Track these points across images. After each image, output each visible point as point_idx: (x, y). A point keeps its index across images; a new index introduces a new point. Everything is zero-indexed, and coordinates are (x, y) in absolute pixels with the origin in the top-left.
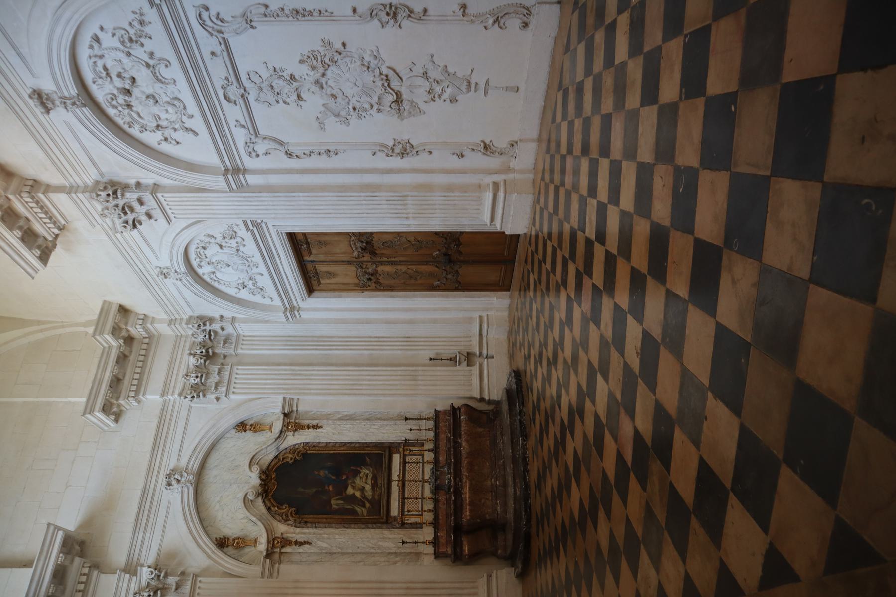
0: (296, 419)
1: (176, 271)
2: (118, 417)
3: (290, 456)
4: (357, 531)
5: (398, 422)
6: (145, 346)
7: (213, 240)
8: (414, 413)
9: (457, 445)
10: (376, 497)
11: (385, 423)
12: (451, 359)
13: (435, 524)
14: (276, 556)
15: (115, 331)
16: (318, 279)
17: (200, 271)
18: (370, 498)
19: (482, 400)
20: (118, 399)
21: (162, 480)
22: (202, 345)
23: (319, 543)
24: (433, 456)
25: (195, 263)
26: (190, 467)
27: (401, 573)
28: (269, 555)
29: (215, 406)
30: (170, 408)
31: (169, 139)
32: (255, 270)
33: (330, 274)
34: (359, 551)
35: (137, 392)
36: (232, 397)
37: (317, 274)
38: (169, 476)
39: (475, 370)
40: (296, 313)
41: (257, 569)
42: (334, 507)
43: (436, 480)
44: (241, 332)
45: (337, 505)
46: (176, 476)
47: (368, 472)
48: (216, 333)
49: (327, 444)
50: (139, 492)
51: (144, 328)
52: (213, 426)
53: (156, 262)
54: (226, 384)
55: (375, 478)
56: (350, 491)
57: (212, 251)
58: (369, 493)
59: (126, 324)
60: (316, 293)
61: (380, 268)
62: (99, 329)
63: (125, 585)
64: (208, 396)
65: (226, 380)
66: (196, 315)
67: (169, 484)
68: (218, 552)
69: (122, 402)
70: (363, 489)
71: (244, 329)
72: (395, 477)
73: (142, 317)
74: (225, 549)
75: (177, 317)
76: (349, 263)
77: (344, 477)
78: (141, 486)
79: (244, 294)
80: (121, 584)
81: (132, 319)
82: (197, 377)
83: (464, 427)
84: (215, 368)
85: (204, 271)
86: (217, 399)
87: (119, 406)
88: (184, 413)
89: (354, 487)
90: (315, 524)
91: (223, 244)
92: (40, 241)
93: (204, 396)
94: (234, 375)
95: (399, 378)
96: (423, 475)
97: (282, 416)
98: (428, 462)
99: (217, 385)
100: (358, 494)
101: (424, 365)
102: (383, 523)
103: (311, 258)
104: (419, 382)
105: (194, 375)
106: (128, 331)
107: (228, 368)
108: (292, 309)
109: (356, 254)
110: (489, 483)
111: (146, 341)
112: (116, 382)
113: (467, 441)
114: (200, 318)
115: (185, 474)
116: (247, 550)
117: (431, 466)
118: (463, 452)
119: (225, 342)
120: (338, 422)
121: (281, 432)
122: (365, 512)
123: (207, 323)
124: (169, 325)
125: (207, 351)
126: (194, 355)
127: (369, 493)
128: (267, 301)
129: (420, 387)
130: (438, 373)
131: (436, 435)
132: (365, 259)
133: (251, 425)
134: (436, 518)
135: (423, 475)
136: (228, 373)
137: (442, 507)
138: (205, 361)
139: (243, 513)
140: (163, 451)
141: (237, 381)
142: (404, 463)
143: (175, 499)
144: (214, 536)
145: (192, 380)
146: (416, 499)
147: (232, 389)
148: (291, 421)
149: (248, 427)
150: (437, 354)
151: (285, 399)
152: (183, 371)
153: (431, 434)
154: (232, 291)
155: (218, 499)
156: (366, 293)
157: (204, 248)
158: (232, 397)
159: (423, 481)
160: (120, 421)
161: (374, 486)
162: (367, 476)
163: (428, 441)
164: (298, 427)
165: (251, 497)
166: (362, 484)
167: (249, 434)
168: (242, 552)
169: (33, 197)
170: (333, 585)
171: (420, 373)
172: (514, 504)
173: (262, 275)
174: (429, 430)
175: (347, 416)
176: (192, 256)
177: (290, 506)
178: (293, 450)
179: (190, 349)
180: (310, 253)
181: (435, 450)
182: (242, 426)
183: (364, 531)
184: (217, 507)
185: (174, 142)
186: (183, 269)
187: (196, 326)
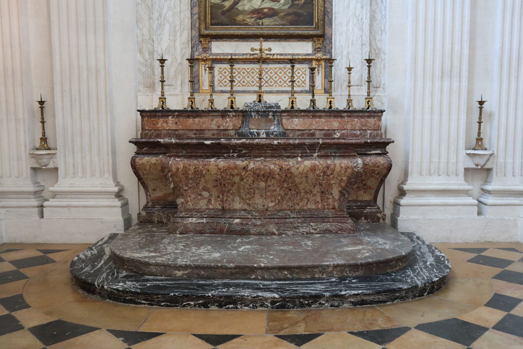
5: (367, 49)
8: (383, 73)
9: (306, 149)
10: (240, 18)
11: (366, 27)
12: (479, 139)
13: (193, 113)
19: (402, 193)
24: (302, 108)
39: (458, 182)
43: (257, 112)
55: (273, 13)
72: (277, 48)
83: (340, 163)
95: (448, 47)
96: (271, 92)
101: (470, 92)
104: (437, 84)
110: (237, 205)
113: (313, 169)
118: (291, 162)
129: (429, 85)
130: (454, 117)
131: (337, 114)
135: (271, 92)
137: (213, 124)
142: (292, 61)
146: (232, 81)
150: (491, 115)
153: (340, 104)
171: (456, 84)
172: (157, 265)
174: (349, 101)
181: (313, 112)
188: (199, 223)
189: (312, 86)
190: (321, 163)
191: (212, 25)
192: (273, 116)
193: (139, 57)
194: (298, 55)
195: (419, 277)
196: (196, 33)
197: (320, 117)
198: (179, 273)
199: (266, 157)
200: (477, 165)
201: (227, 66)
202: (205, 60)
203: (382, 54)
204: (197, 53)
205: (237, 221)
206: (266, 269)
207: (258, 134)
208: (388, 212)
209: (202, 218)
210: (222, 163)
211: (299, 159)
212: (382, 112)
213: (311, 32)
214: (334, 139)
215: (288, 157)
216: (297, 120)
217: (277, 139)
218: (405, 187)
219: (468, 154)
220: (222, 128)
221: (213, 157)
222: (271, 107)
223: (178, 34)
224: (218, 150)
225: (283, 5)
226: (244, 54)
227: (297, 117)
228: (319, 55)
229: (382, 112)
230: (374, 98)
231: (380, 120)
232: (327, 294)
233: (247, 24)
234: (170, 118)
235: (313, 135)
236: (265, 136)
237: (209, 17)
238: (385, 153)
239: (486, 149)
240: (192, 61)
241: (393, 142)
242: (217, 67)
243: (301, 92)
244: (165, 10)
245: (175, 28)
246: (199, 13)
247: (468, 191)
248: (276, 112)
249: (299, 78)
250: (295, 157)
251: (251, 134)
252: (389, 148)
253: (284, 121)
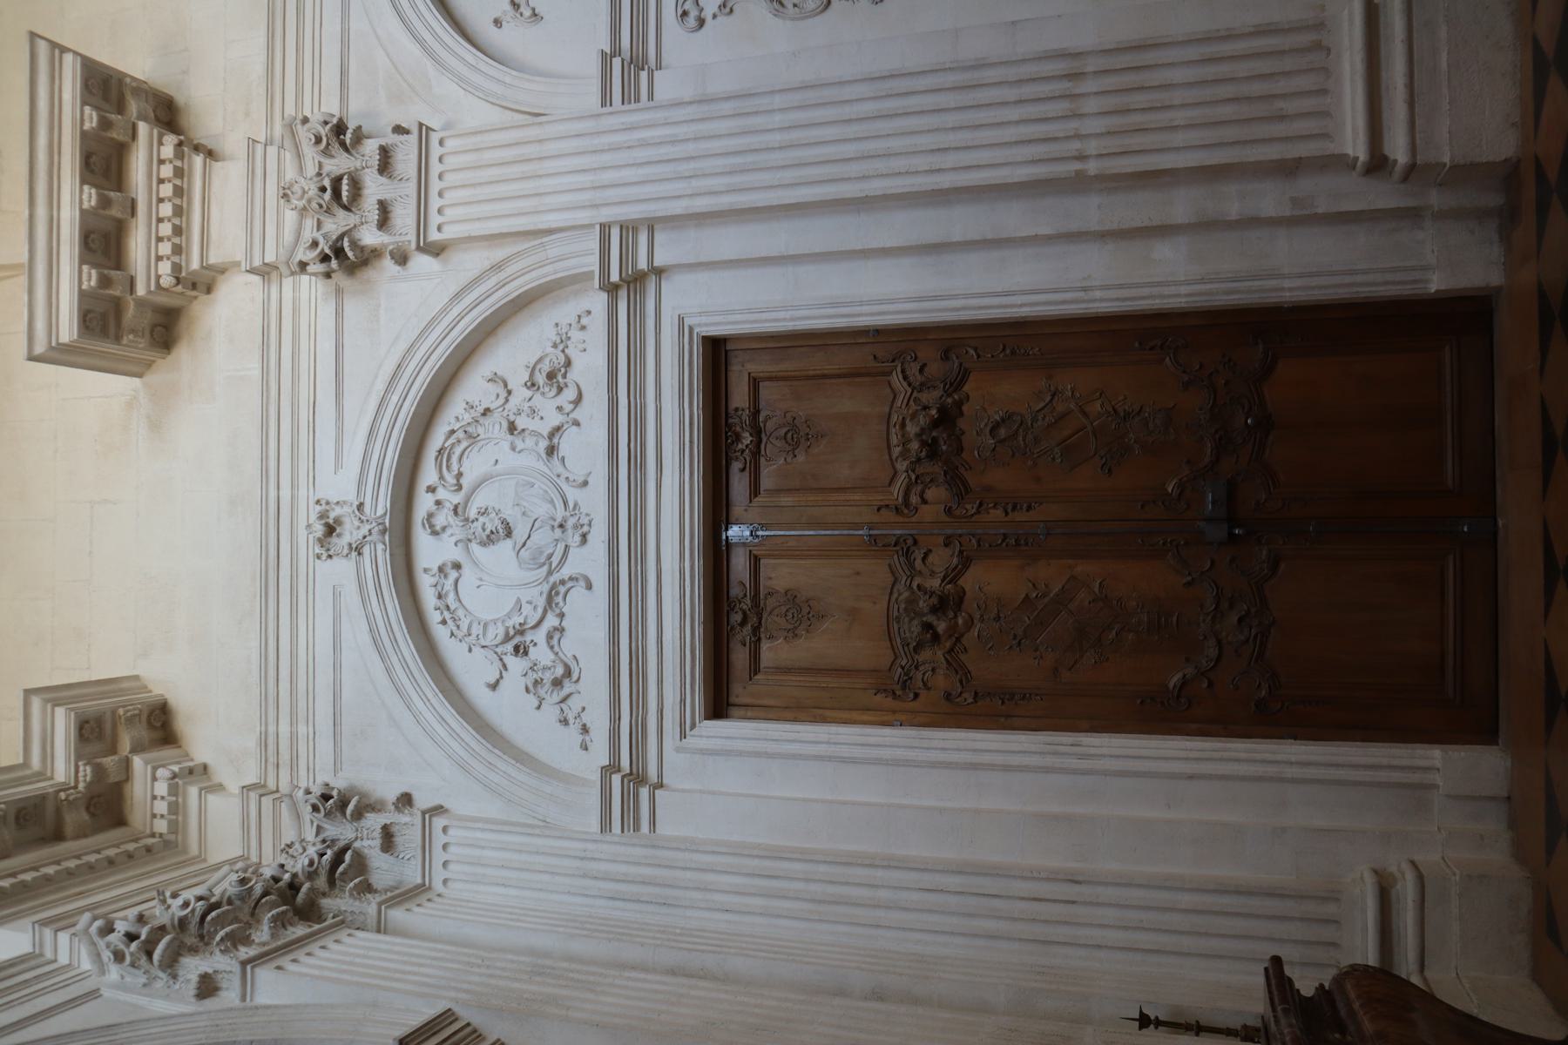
31: (522, 9)
81: (167, 753)
91: (521, 423)
106: (127, 764)
108: (637, 777)
169: (179, 154)
185: (527, 13)
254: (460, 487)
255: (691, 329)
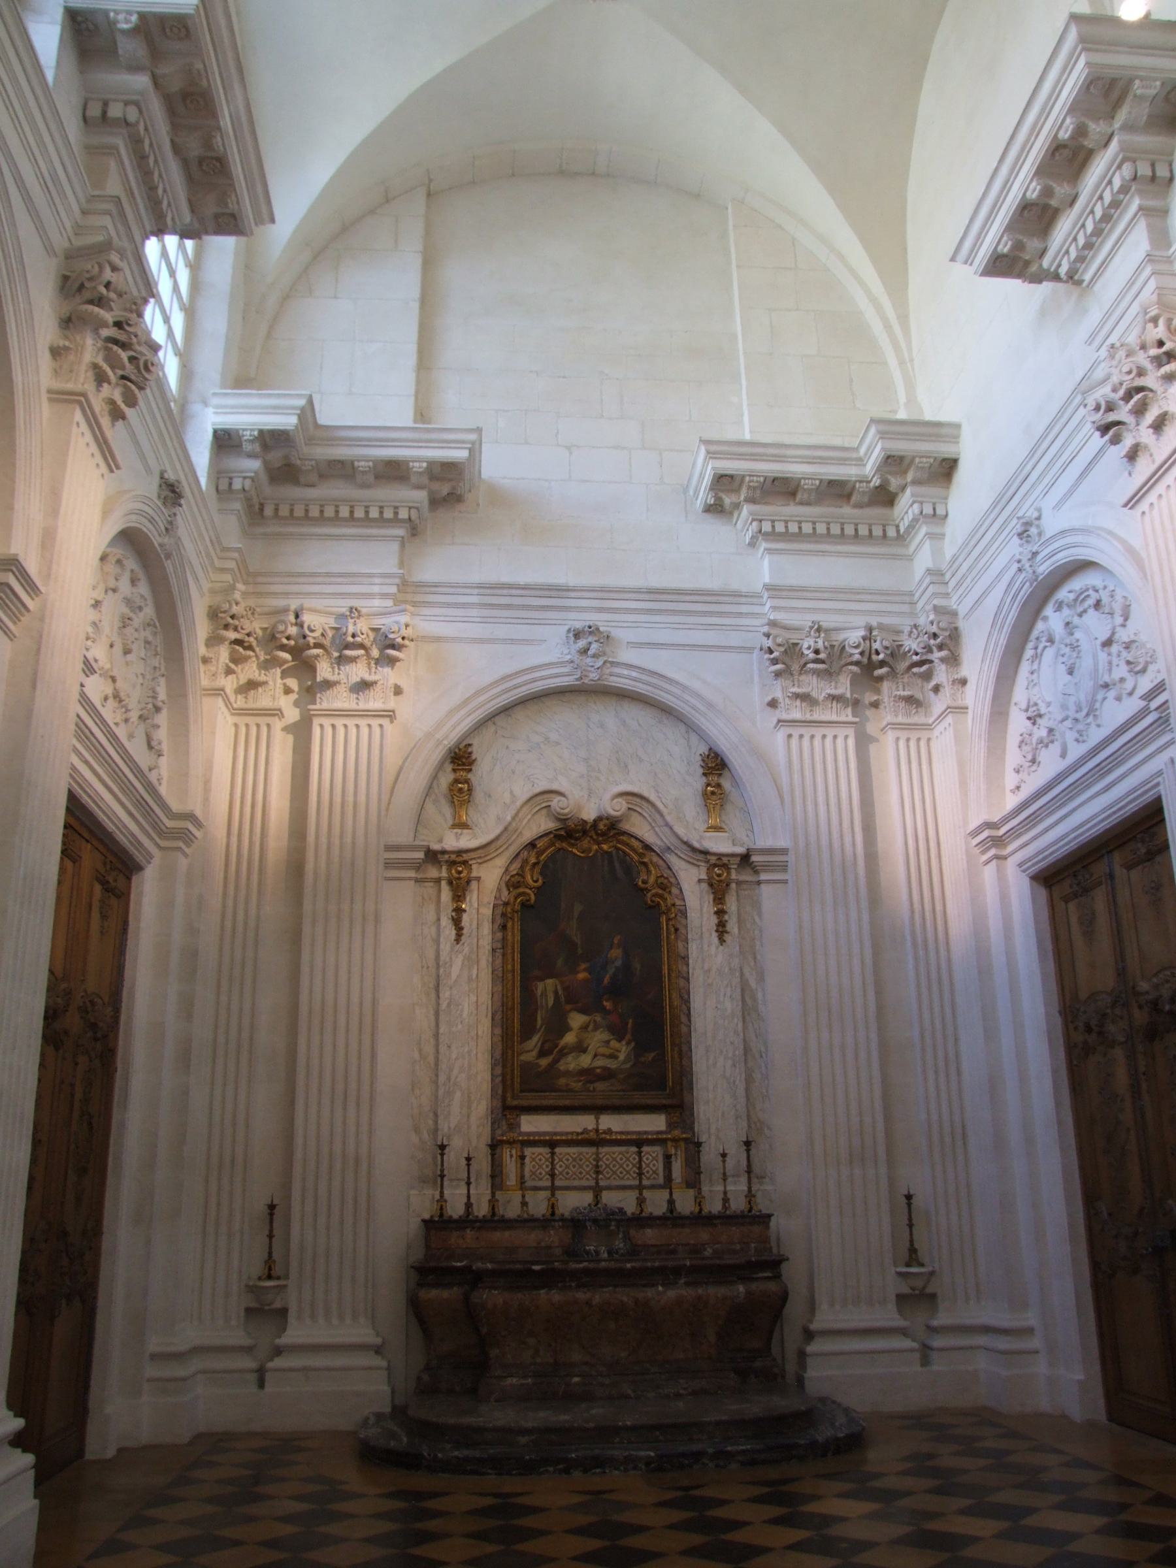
0: (739, 883)
1: (1035, 554)
2: (715, 509)
3: (652, 879)
4: (485, 1042)
5: (744, 1124)
6: (878, 531)
7: (1119, 620)
9: (669, 1275)
10: (562, 1081)
11: (741, 1092)
12: (913, 1251)
14: (433, 872)
15: (894, 462)
16: (1076, 895)
17: (1049, 611)
18: (562, 1066)
19: (809, 1335)
20: (751, 500)
21: (579, 620)
22: (895, 653)
23: (458, 962)
25: (1063, 594)
26: (617, 670)
27: (393, 1146)
28: (432, 856)
29: (758, 698)
30: (744, 609)
32: (1070, 736)
33: (1088, 923)
34: (443, 1049)
35: (772, 536)
36: (781, 735)
37: (1086, 891)
38: (593, 630)
39: (889, 1316)
40: (993, 852)
41: (404, 836)
42: (540, 986)
43: (595, 1221)
44: (936, 732)
45: (544, 994)
46: (594, 646)
47: (622, 1057)
48: (928, 676)
49: (685, 959)
50: (560, 579)
51: (915, 520)
52: (710, 705)
53: (1047, 504)
54: (808, 717)
55: (608, 1075)
56: (577, 1020)
57: (1095, 626)
58: (571, 1063)
59: (916, 482)
60: (1043, 893)
61: (1119, 1053)
62: (888, 427)
63: (376, 589)
64: (779, 683)
65: (816, 716)
66: (961, 624)
67: (577, 635)
68: (438, 754)
69: (746, 509)
70: (581, 1048)
71: (943, 738)
73: (940, 511)
74: (449, 767)
75: (952, 584)
76: (1121, 972)
77: (608, 1005)
78: (572, 582)
79: (1017, 722)
80: (377, 580)
82: (817, 652)
83: (715, 1292)
84: (843, 686)
85: (1053, 620)
86: (773, 704)
87: (737, 506)
88: (735, 639)
89: (584, 1028)
90: (501, 948)
91: (1115, 648)
92: (1033, 244)
93: (778, 674)
94: (830, 732)
97: (740, 850)
98: (641, 1201)
99: (804, 698)
100: (569, 1038)
101: (892, 1181)
102: (504, 1099)
103: (1119, 871)
105: (820, 645)
106: (903, 488)
107: (847, 715)
109: (1144, 986)
111: (891, 532)
112: (783, 489)
114: (955, 635)
115: (599, 663)
116: (447, 811)
117: (631, 1208)
118: (650, 1293)
119: (910, 700)
120: (736, 981)
121: (706, 853)
122: (529, 1057)
123: (944, 653)
124: (929, 571)
125: (882, 664)
126: (868, 638)
127: (571, 1063)
128: (1011, 779)
132: (1136, 1012)
133: (719, 786)
134: (507, 1224)
136: (834, 718)
138: (857, 663)
139: (523, 791)
140: (649, 611)
141: (817, 742)
142: (640, 1142)
143: (547, 652)
144: (475, 742)
145: (807, 644)
147: (796, 732)
148: (730, 874)
149: (714, 779)
151: (784, 851)
152: (828, 621)
154: (1020, 695)
155: (554, 736)
156: (1058, 1021)
157: (1098, 605)
158: (781, 735)
159: (597, 1190)
160: (707, 515)
161: (588, 1074)
162: (613, 1056)
163: (699, 1200)
164: (718, 890)
165: (556, 803)
166: (592, 1044)
167: (698, 782)
168: (443, 802)
170: (368, 996)
173: (1063, 755)
175: (754, 999)
176: (1077, 583)
177: (539, 891)
178: (667, 884)
179: (881, 627)
180: (1129, 867)
181: (672, 1218)
182: (715, 765)
183: (488, 1056)
184: (536, 739)
186: (1044, 569)
187: (934, 629)
188: (522, 1385)
189: (668, 1178)
190: (688, 1293)
191: (522, 1091)
192: (618, 1227)
193: (415, 1139)
194: (646, 1133)
195: (823, 1434)
196: (498, 1104)
197: (683, 1226)
198: (523, 1440)
199: (616, 1286)
200: (913, 1289)
201: (544, 1151)
202: (511, 1143)
203: (766, 1131)
204: (499, 1132)
205: (576, 1379)
206: (633, 1428)
207: (597, 1253)
208: (791, 1367)
209: (525, 1377)
210: (556, 1296)
211: (660, 1288)
212: (769, 1216)
213: (664, 1102)
214: (703, 1259)
215: (644, 1286)
216: (649, 1230)
217: (629, 1261)
218: (814, 1327)
219: (899, 1274)
220: (543, 1244)
221: (543, 1288)
222: (613, 1213)
223: (474, 1105)
224: (550, 1278)
225: (624, 1062)
226: (567, 1133)
227: (650, 1226)
228: (676, 1133)
229: (769, 1216)
230: (759, 1194)
231: (767, 1226)
232: (711, 1451)
233: (571, 1090)
234: (468, 1231)
235: (674, 1252)
236: (606, 1255)
237: (517, 1080)
238: (777, 1277)
239: (922, 1265)
240: (495, 1146)
241: (787, 1259)
242: (528, 1151)
243: (653, 1187)
244: (455, 1072)
245: (469, 1097)
246: (504, 1075)
247: (904, 1329)
248: (622, 1220)
249: (648, 1165)
250: (653, 1285)
251: (588, 1253)
252: (784, 1267)
253: (632, 1232)
254: (1080, 615)
255: (1158, 784)
